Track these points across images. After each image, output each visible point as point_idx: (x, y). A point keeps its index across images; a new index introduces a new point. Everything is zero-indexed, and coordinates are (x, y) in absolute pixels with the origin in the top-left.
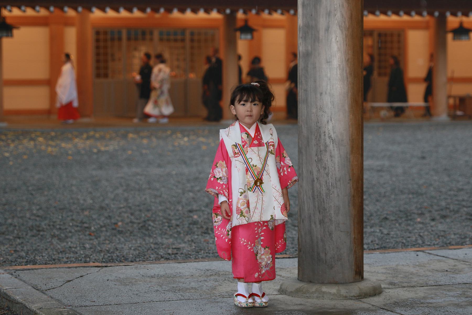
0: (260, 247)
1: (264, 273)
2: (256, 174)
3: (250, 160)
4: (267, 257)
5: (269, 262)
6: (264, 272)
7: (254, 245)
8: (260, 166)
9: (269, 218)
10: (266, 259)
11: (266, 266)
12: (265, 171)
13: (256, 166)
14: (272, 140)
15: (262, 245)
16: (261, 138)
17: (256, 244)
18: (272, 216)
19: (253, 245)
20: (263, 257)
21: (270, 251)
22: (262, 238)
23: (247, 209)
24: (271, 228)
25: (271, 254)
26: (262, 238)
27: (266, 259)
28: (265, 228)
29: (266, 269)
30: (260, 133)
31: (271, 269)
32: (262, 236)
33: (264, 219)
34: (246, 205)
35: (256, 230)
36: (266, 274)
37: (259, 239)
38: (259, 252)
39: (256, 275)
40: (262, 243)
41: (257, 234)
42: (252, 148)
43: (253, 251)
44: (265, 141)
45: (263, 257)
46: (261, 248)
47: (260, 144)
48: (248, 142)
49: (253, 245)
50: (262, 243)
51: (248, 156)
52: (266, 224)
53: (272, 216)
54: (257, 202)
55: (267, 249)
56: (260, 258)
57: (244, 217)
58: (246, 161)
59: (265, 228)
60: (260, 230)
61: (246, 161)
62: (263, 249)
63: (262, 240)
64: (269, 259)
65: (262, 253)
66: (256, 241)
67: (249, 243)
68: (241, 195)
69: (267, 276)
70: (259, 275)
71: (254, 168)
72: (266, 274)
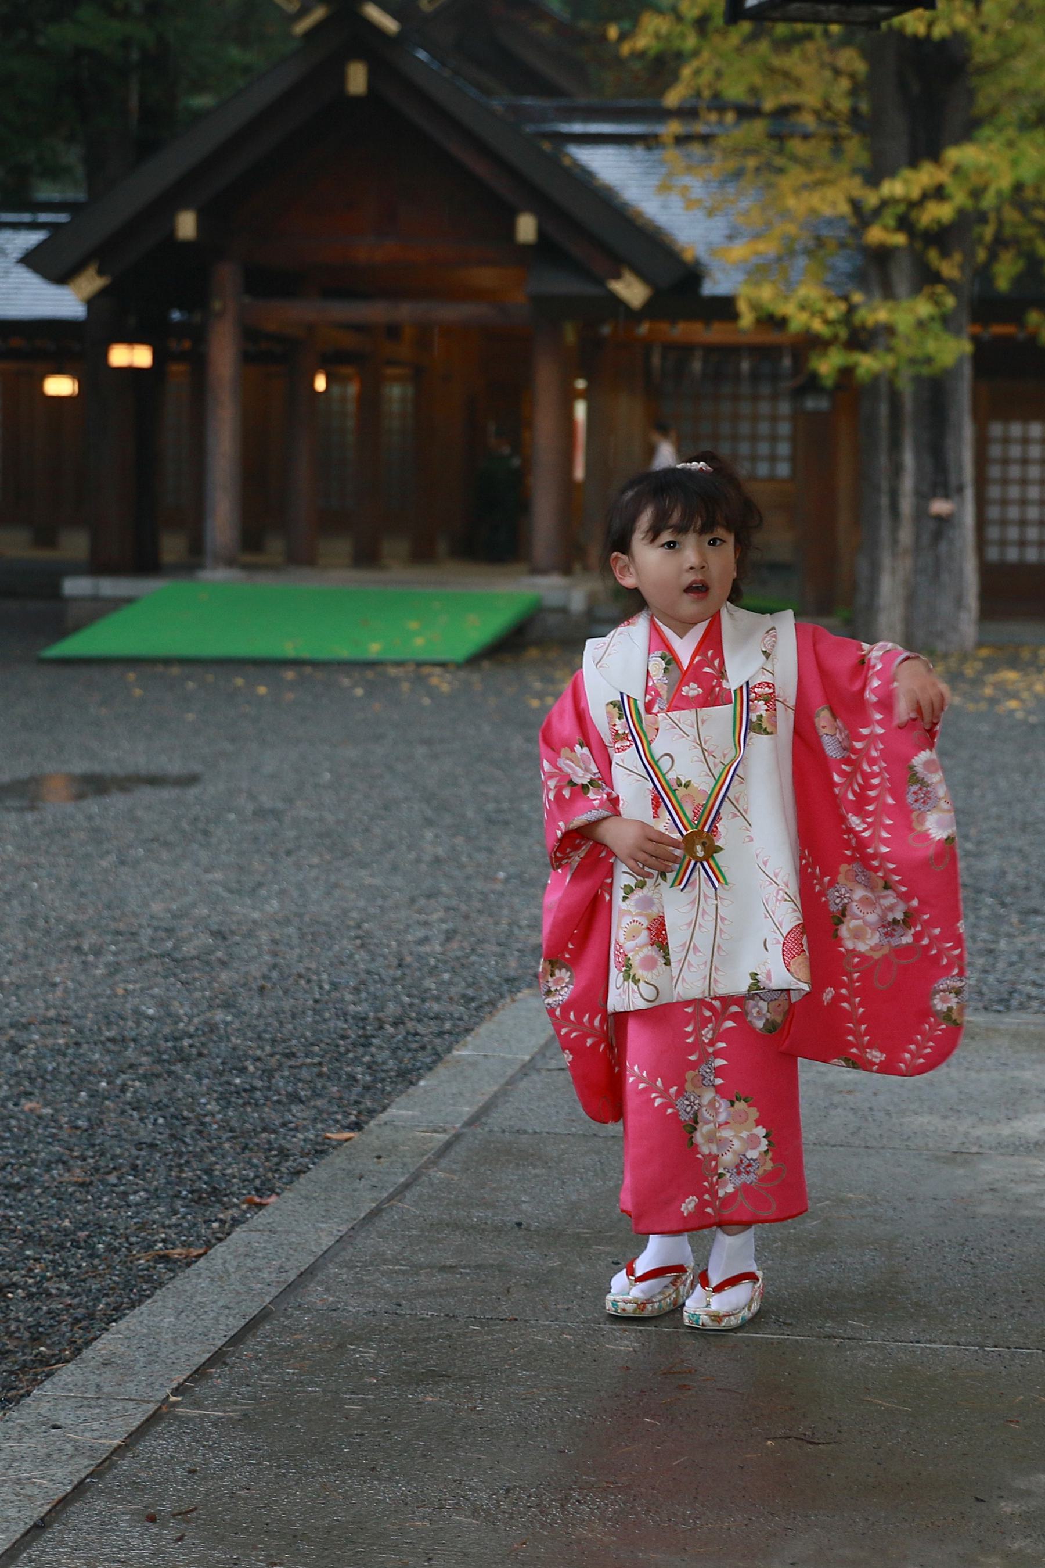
0: (709, 1095)
1: (730, 1198)
2: (690, 815)
3: (665, 764)
4: (744, 1134)
5: (752, 1154)
6: (730, 1189)
7: (681, 1093)
8: (703, 783)
9: (742, 986)
10: (737, 1144)
11: (741, 1166)
12: (726, 803)
13: (687, 786)
14: (767, 678)
15: (718, 1089)
16: (722, 674)
17: (688, 1086)
18: (754, 975)
19: (673, 1090)
20: (726, 1133)
21: (754, 1113)
22: (720, 1062)
23: (651, 951)
24: (760, 1024)
25: (758, 1123)
26: (720, 1062)
27: (737, 1144)
28: (729, 1024)
29: (739, 1181)
30: (719, 653)
31: (761, 1179)
32: (717, 1054)
33: (722, 990)
34: (644, 936)
35: (689, 1035)
36: (741, 1197)
37: (704, 1069)
38: (705, 1114)
39: (689, 1205)
40: (719, 1081)
41: (692, 1048)
42: (675, 715)
43: (676, 1115)
44: (734, 681)
45: (726, 1133)
46: (712, 1104)
47: (712, 697)
48: (664, 693)
49: (673, 1090)
50: (719, 1081)
51: (658, 748)
52: (735, 1009)
53: (754, 975)
54: (694, 924)
55: (740, 1105)
56: (711, 1139)
57: (636, 982)
58: (651, 765)
59: (729, 1024)
60: (707, 1034)
61: (651, 765)
62: (723, 1104)
63: (718, 1072)
64: (753, 1142)
65: (722, 1117)
66: (690, 1075)
67: (659, 1083)
68: (625, 899)
69: (746, 1204)
70: (701, 1205)
71: (681, 792)
72: (741, 1197)
